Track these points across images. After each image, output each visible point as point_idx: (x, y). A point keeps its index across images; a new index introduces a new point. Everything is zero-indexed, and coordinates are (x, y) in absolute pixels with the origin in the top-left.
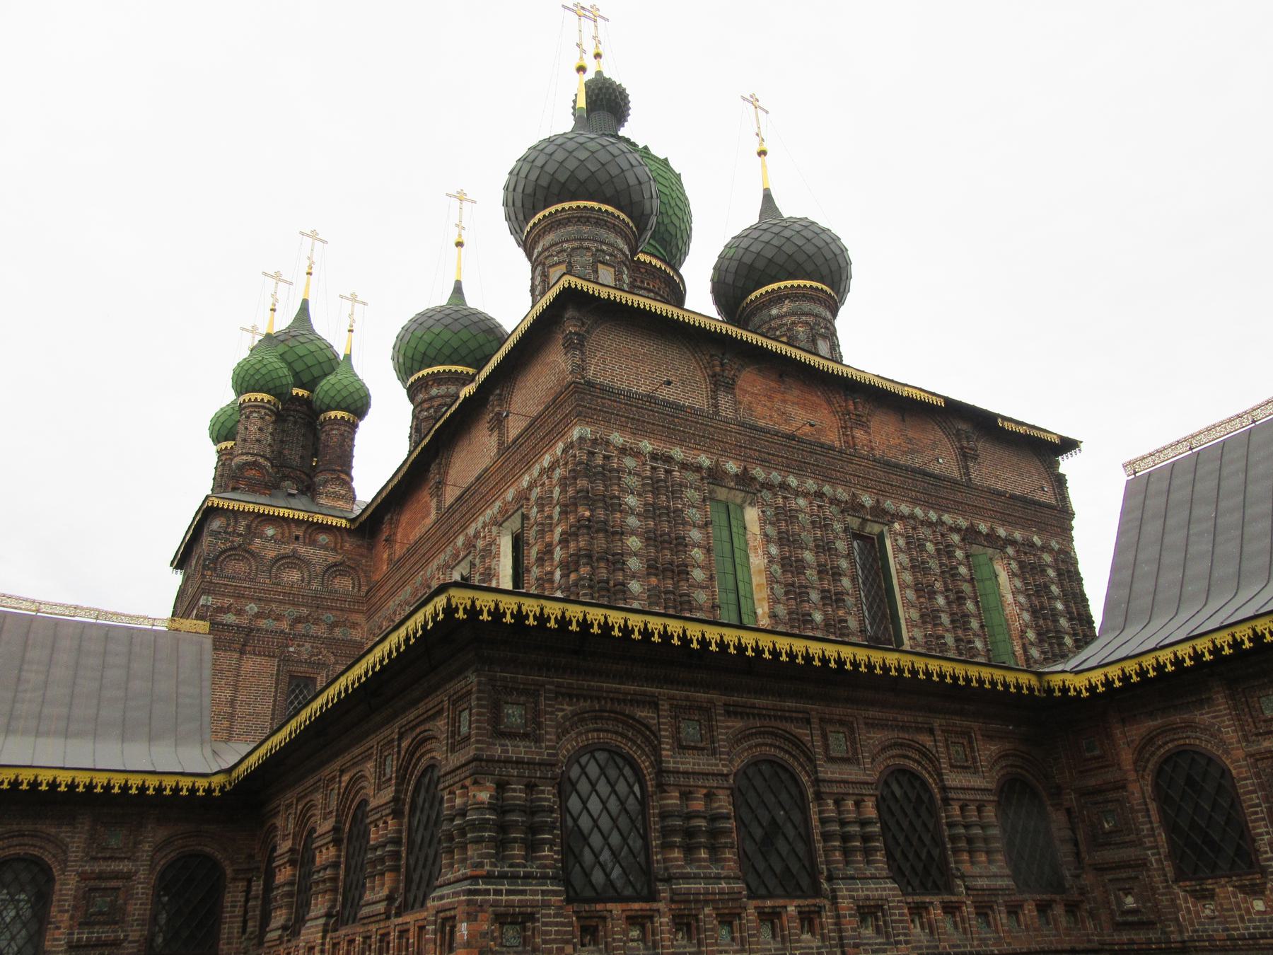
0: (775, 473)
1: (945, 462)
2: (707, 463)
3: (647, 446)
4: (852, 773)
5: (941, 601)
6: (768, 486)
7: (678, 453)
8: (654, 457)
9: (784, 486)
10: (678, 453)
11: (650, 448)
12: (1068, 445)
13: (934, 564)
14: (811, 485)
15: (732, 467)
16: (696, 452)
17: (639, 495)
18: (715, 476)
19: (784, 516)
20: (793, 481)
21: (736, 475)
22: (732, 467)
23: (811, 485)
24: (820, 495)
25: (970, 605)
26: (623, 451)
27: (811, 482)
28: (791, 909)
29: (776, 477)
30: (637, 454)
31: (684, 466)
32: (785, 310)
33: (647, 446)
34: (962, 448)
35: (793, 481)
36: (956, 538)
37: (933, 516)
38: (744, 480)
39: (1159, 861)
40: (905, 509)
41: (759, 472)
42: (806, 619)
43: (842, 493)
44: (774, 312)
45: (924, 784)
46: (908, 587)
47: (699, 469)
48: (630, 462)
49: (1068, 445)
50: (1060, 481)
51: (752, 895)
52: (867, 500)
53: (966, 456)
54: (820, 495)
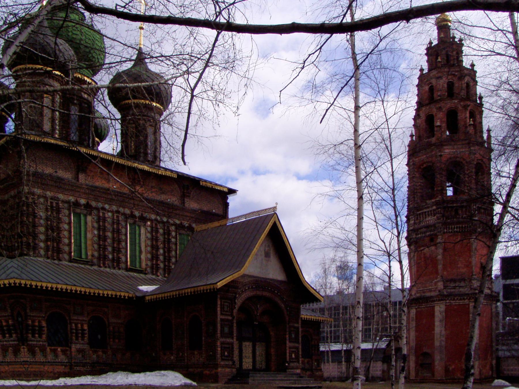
0: (100, 204)
1: (173, 199)
5: (161, 251)
6: (97, 209)
7: (61, 196)
9: (103, 209)
10: (61, 196)
12: (232, 191)
13: (161, 238)
14: (114, 208)
15: (83, 201)
19: (101, 220)
20: (107, 206)
21: (84, 204)
22: (83, 201)
23: (114, 208)
24: (118, 212)
25: (173, 253)
26: (39, 197)
27: (114, 207)
28: (59, 349)
29: (100, 205)
30: (45, 197)
34: (184, 193)
35: (107, 206)
36: (173, 228)
37: (165, 219)
38: (88, 206)
40: (153, 217)
41: (93, 204)
42: (105, 257)
43: (127, 211)
46: (148, 246)
49: (232, 191)
50: (227, 205)
51: (49, 345)
52: (137, 214)
53: (183, 197)
54: (118, 212)
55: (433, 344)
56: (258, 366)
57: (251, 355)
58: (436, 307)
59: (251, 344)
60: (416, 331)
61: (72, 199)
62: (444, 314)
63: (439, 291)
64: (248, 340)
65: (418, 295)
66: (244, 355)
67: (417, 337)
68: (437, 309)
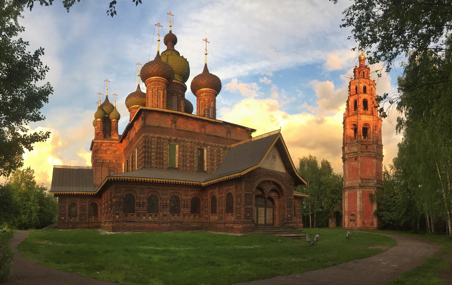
2: (169, 138)
3: (157, 136)
4: (166, 197)
7: (163, 136)
8: (158, 138)
10: (163, 136)
11: (157, 136)
16: (167, 136)
17: (155, 145)
18: (170, 140)
31: (163, 139)
32: (204, 95)
33: (157, 136)
39: (209, 211)
44: (201, 95)
45: (179, 198)
47: (167, 139)
48: (153, 139)
55: (356, 209)
56: (267, 222)
57: (264, 215)
58: (357, 191)
59: (264, 209)
60: (348, 203)
61: (168, 137)
62: (362, 195)
63: (359, 184)
64: (261, 206)
65: (349, 185)
66: (259, 215)
67: (349, 207)
68: (358, 192)
